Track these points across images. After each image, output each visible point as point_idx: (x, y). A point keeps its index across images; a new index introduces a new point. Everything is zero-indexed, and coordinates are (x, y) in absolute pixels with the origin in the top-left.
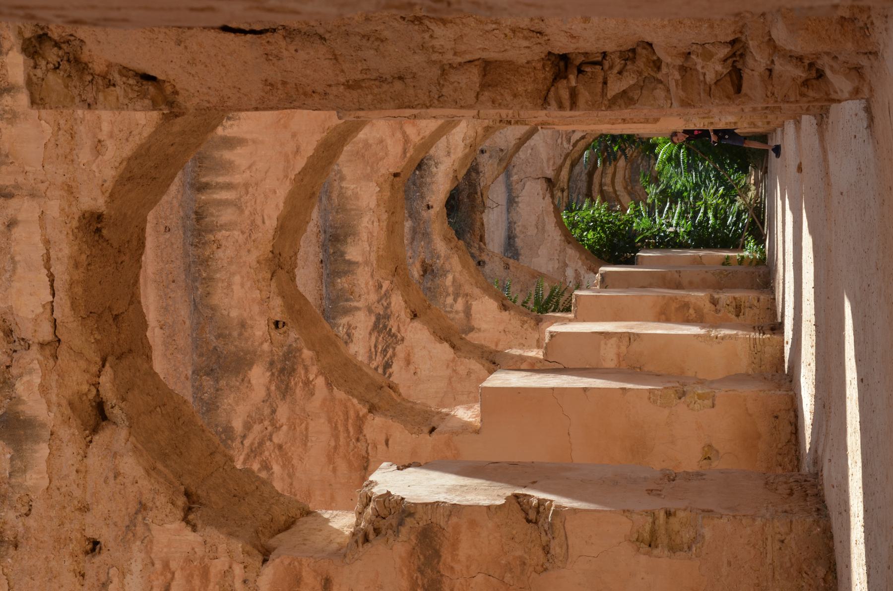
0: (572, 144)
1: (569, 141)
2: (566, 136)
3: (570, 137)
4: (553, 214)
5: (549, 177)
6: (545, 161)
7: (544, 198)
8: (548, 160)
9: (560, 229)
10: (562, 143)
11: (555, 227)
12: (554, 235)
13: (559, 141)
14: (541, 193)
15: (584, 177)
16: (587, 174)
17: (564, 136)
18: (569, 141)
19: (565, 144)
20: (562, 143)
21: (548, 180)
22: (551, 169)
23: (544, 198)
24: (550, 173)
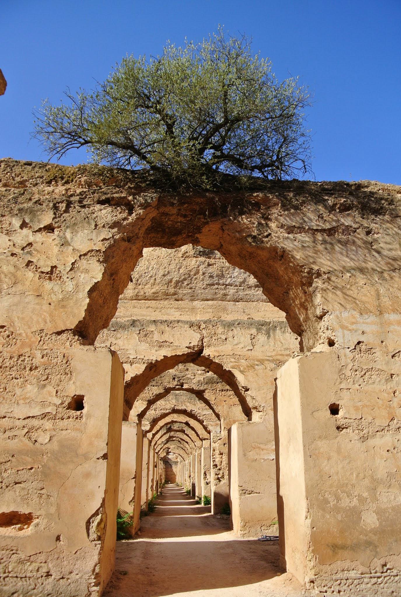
0: (230, 369)
1: (233, 367)
2: (237, 366)
3: (236, 369)
4: (174, 354)
5: (204, 352)
6: (217, 349)
7: (187, 347)
8: (218, 352)
9: (161, 360)
10: (231, 362)
11: (164, 356)
12: (157, 355)
13: (233, 360)
14: (192, 345)
15: (184, 407)
16: (185, 410)
17: (237, 364)
18: (233, 367)
19: (232, 364)
20: (231, 362)
21: (201, 351)
22: (211, 354)
23: (187, 347)
24: (206, 352)
